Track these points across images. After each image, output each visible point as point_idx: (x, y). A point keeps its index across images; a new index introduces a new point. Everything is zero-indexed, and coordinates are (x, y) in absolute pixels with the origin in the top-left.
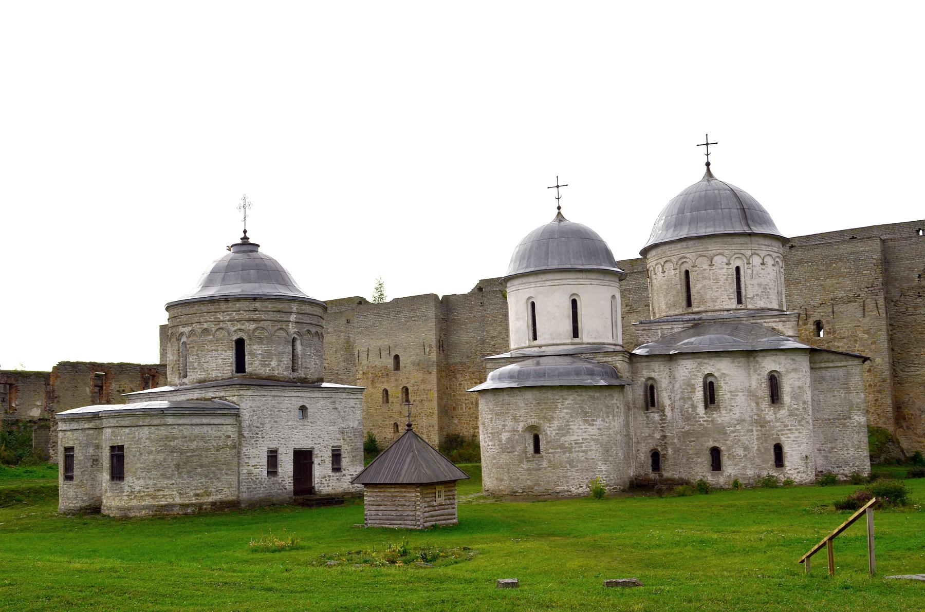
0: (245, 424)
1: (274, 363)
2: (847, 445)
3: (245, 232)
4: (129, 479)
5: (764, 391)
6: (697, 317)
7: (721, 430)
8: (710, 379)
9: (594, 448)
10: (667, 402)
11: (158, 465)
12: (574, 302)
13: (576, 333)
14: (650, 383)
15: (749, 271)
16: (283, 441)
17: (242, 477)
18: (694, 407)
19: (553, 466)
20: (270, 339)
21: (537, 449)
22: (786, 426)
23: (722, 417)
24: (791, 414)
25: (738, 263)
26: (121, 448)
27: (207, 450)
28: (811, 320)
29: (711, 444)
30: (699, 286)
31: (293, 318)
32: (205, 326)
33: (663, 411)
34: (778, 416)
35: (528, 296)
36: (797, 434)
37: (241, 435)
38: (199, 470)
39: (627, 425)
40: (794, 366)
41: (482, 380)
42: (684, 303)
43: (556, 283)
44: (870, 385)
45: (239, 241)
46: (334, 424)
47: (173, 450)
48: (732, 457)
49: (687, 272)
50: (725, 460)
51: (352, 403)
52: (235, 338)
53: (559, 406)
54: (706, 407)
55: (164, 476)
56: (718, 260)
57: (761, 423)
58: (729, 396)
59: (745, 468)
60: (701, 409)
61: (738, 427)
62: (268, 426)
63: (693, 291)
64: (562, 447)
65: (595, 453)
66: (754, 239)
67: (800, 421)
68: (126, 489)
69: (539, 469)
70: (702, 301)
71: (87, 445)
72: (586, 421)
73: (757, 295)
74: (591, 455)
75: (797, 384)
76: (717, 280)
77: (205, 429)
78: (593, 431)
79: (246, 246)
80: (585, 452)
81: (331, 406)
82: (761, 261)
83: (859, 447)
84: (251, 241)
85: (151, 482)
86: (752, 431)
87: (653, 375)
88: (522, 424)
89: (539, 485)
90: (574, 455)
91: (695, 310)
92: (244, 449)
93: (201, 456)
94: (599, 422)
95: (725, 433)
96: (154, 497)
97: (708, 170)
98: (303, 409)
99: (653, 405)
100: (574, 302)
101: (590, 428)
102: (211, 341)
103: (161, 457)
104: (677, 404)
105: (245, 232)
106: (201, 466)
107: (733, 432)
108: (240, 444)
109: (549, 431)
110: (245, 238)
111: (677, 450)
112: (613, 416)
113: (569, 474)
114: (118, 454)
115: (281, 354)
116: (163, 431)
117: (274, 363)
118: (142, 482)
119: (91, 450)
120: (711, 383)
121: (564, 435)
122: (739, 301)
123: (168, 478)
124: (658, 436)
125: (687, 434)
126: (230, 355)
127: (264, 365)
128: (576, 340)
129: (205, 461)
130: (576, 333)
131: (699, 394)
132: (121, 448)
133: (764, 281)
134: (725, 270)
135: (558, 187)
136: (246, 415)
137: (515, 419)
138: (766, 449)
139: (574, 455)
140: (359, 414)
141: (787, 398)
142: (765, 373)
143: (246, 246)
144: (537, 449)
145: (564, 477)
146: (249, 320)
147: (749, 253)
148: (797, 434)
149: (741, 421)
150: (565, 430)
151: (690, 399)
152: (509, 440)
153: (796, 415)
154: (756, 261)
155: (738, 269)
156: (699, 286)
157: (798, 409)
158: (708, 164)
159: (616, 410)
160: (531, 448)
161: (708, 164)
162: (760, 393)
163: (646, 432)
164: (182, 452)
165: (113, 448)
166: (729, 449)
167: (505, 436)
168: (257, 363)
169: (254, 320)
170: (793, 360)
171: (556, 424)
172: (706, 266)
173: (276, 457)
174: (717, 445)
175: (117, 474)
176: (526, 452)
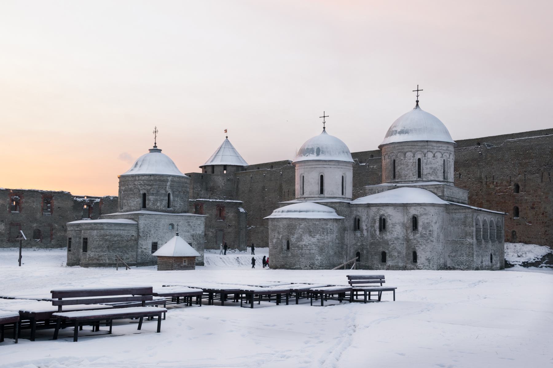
2: (463, 254)
3: (155, 143)
4: (89, 252)
5: (410, 224)
6: (394, 185)
7: (386, 243)
8: (383, 217)
9: (314, 248)
10: (365, 228)
11: (100, 246)
12: (322, 177)
13: (322, 191)
14: (357, 218)
15: (425, 161)
16: (160, 239)
17: (139, 253)
18: (375, 231)
19: (293, 256)
20: (157, 194)
21: (288, 248)
22: (419, 242)
23: (388, 236)
24: (422, 236)
25: (419, 156)
26: (87, 239)
27: (123, 241)
28: (513, 183)
29: (381, 249)
30: (399, 168)
31: (169, 184)
32: (130, 187)
33: (362, 231)
34: (415, 237)
35: (301, 172)
36: (424, 247)
37: (139, 235)
38: (118, 249)
39: (342, 238)
40: (425, 212)
41: (269, 215)
42: (392, 177)
43: (313, 166)
44: (543, 222)
45: (152, 148)
46: (188, 232)
47: (106, 240)
48: (391, 256)
49: (394, 161)
50: (388, 258)
51: (199, 222)
52: (142, 192)
53: (298, 227)
54: (380, 230)
55: (102, 251)
56: (409, 154)
57: (408, 240)
58: (391, 226)
59: (398, 262)
60: (378, 232)
61: (395, 242)
62: (152, 232)
63: (396, 170)
64: (298, 247)
65: (315, 250)
66: (429, 143)
67: (426, 240)
68: (88, 256)
69: (287, 257)
70: (400, 176)
71: (76, 237)
72: (311, 235)
73: (429, 173)
74: (312, 251)
75: (426, 221)
76: (407, 165)
78: (314, 240)
80: (310, 250)
81: (187, 224)
82: (433, 155)
83: (469, 255)
84: (158, 148)
85: (97, 253)
86: (403, 244)
87: (358, 214)
88: (281, 236)
89: (287, 264)
90: (304, 251)
91: (397, 181)
92: (140, 241)
93: (119, 243)
94: (318, 236)
95: (388, 244)
96: (98, 260)
97: (417, 105)
98: (172, 225)
99: (359, 228)
100: (322, 177)
101: (312, 239)
102: (132, 194)
103: (101, 243)
104: (370, 229)
105: (155, 143)
106: (119, 247)
107: (392, 244)
108: (138, 239)
109: (293, 240)
110: (155, 147)
111: (368, 252)
112: (327, 233)
113: (301, 260)
114: (85, 241)
115: (162, 200)
116: (102, 232)
117: (158, 204)
118: (93, 253)
119: (78, 240)
120: (384, 219)
121: (299, 241)
122: (419, 176)
123: (104, 252)
124: (359, 244)
125: (372, 244)
126: (140, 200)
127: (153, 204)
128: (322, 196)
129: (121, 246)
130: (322, 191)
131: (377, 224)
132: (87, 239)
133: (434, 166)
134: (411, 161)
135: (324, 117)
136: (141, 226)
137: (279, 233)
138: (409, 254)
139: (304, 251)
140: (202, 227)
141: (420, 228)
142: (411, 216)
144: (288, 248)
145: (298, 261)
146: (148, 185)
147: (426, 150)
148: (424, 247)
149: (397, 239)
150: (300, 239)
151: (374, 226)
152: (276, 243)
153: (425, 237)
154: (430, 155)
155: (419, 160)
156: (399, 168)
157: (426, 234)
158: (417, 101)
159: (329, 230)
160: (285, 247)
161: (417, 101)
162: (408, 225)
163: (354, 242)
164: (110, 241)
165: (84, 239)
166: (389, 253)
167: (275, 241)
168: (151, 204)
169: (150, 185)
170: (425, 209)
171: (296, 236)
172: (402, 158)
173: (157, 246)
174: (384, 250)
175: (85, 249)
176: (282, 249)
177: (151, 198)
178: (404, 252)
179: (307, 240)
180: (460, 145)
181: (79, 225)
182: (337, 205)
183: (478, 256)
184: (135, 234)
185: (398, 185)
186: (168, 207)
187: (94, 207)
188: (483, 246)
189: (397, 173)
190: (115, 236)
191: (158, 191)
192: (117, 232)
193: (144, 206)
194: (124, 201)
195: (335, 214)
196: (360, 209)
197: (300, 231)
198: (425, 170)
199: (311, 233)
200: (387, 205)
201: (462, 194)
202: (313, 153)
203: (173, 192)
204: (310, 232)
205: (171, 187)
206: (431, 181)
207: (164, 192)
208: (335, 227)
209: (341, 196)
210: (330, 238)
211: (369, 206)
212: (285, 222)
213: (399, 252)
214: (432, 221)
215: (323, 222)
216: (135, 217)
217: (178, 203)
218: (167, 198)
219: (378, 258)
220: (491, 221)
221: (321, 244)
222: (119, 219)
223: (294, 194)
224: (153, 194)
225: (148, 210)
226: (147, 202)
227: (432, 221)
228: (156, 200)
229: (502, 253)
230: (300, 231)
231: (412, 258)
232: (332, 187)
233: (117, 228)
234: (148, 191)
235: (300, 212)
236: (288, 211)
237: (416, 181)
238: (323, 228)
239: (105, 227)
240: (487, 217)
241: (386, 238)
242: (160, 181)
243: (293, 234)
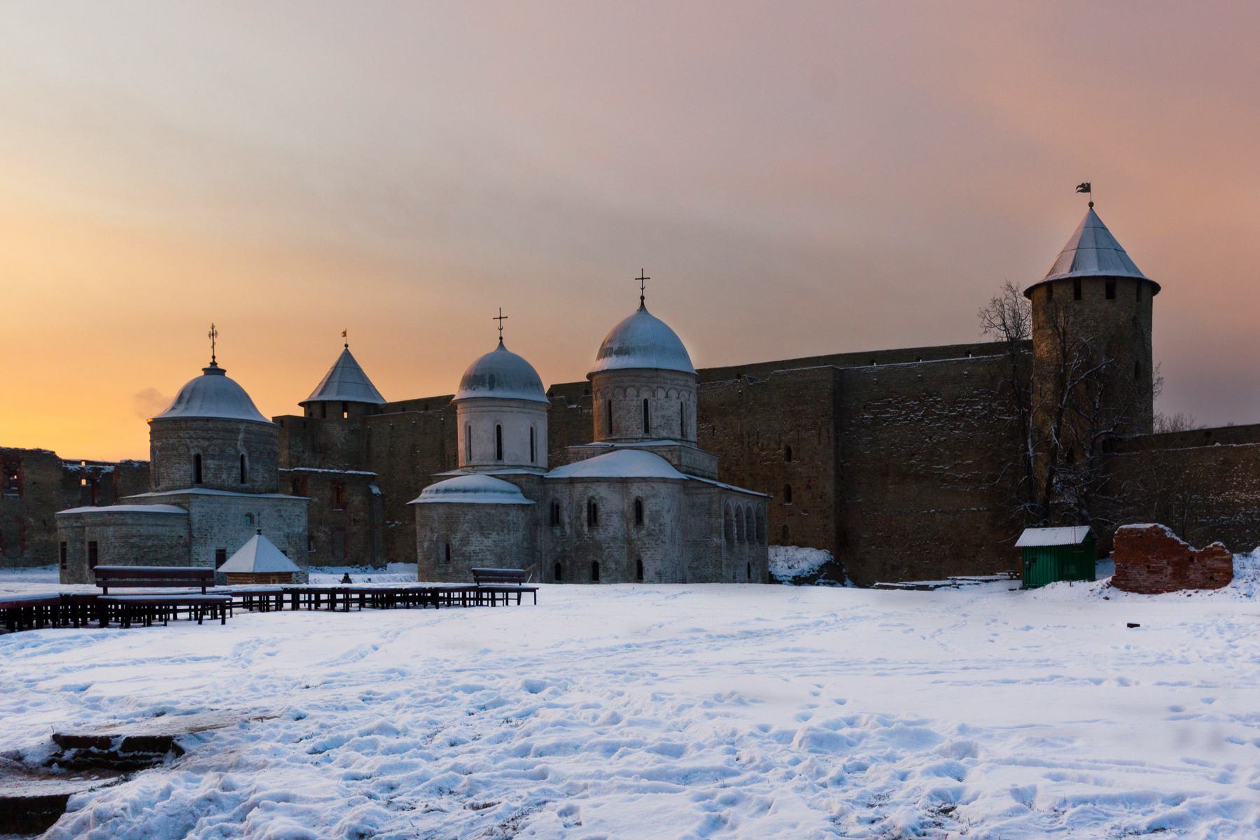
0: (195, 526)
1: (224, 476)
7: (598, 546)
12: (499, 428)
18: (582, 526)
23: (600, 535)
27: (163, 546)
29: (591, 558)
32: (171, 441)
37: (191, 536)
45: (208, 366)
47: (132, 546)
48: (606, 570)
52: (193, 453)
54: (590, 525)
60: (586, 528)
72: (482, 534)
77: (160, 529)
79: (214, 370)
84: (219, 366)
94: (494, 536)
100: (499, 428)
103: (123, 551)
110: (214, 364)
115: (231, 468)
116: (124, 529)
117: (224, 476)
122: (647, 430)
126: (189, 468)
129: (160, 556)
131: (585, 514)
136: (195, 518)
143: (214, 370)
150: (465, 541)
171: (459, 535)
177: (210, 463)
178: (625, 561)
179: (478, 543)
180: (706, 376)
181: (79, 516)
182: (524, 479)
183: (728, 566)
184: (183, 533)
185: (617, 445)
186: (243, 481)
187: (105, 481)
188: (736, 550)
189: (614, 425)
190: (149, 537)
191: (222, 451)
192: (153, 530)
193: (198, 480)
194: (162, 470)
195: (520, 495)
196: (559, 487)
197: (465, 527)
198: (655, 422)
199: (483, 531)
200: (598, 480)
201: (708, 463)
202: (483, 385)
203: (250, 453)
204: (482, 528)
205: (247, 442)
206: (664, 439)
207: (233, 452)
208: (519, 518)
209: (529, 463)
210: (513, 539)
211: (572, 481)
212: (441, 510)
213: (617, 563)
214: (661, 506)
215: (502, 510)
216: (181, 501)
217: (259, 475)
218: (239, 464)
219: (587, 572)
220: (749, 509)
221: (499, 550)
222: (153, 504)
223: (456, 460)
224: (213, 457)
225: (206, 487)
226: (203, 472)
227: (661, 506)
228: (219, 468)
229: (765, 560)
230: (465, 527)
231: (635, 572)
232: (516, 448)
233: (151, 521)
234: (205, 450)
235: (465, 491)
236: (447, 491)
237: (643, 439)
238: (502, 521)
239: (130, 521)
240: (742, 499)
241: (598, 538)
242: (227, 431)
243: (455, 532)
